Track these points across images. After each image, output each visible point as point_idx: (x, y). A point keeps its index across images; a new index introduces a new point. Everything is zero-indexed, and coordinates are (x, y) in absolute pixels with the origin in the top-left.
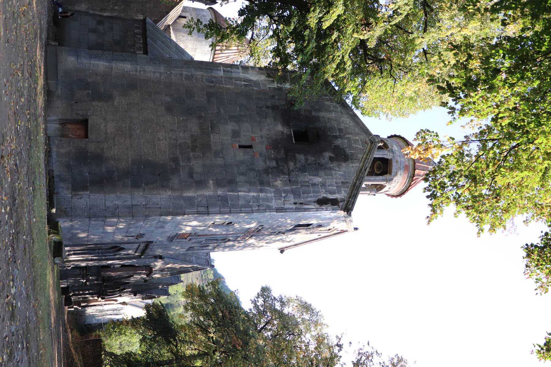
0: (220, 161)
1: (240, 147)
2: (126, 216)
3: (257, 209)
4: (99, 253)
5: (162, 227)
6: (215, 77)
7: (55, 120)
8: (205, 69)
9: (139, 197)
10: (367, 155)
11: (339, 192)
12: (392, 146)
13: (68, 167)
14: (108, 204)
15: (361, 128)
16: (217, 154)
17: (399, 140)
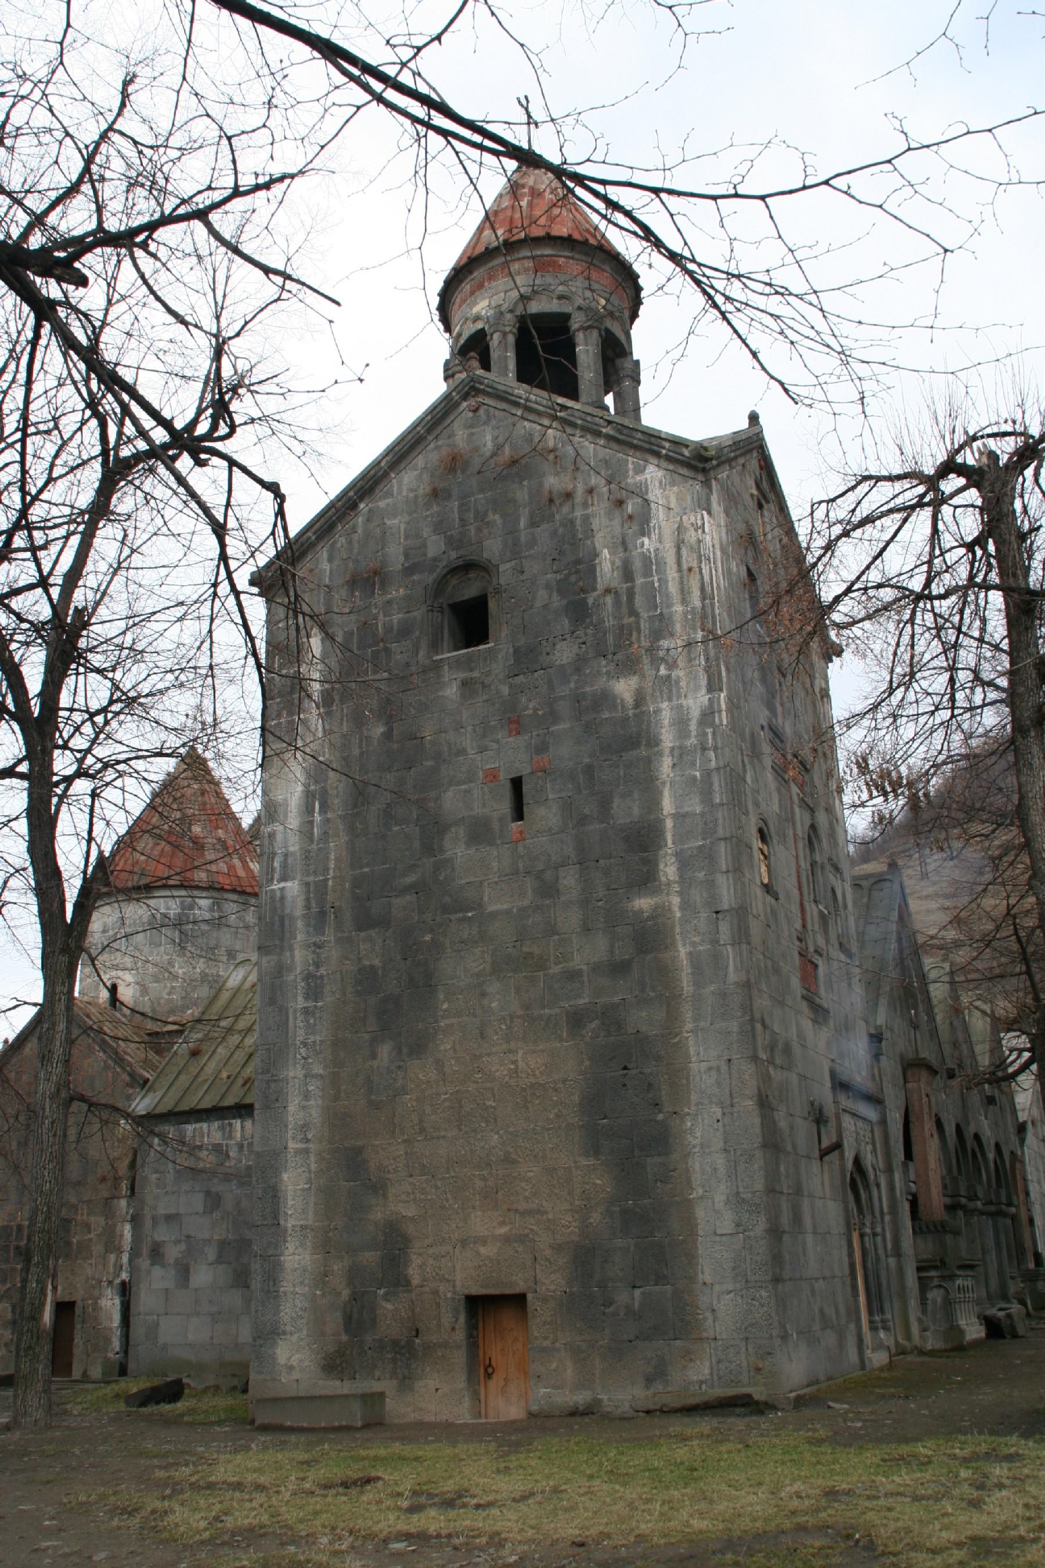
0: (569, 880)
1: (519, 814)
3: (712, 754)
4: (875, 1235)
5: (787, 1050)
6: (308, 907)
8: (282, 939)
12: (477, 318)
14: (726, 1225)
15: (429, 431)
16: (548, 890)
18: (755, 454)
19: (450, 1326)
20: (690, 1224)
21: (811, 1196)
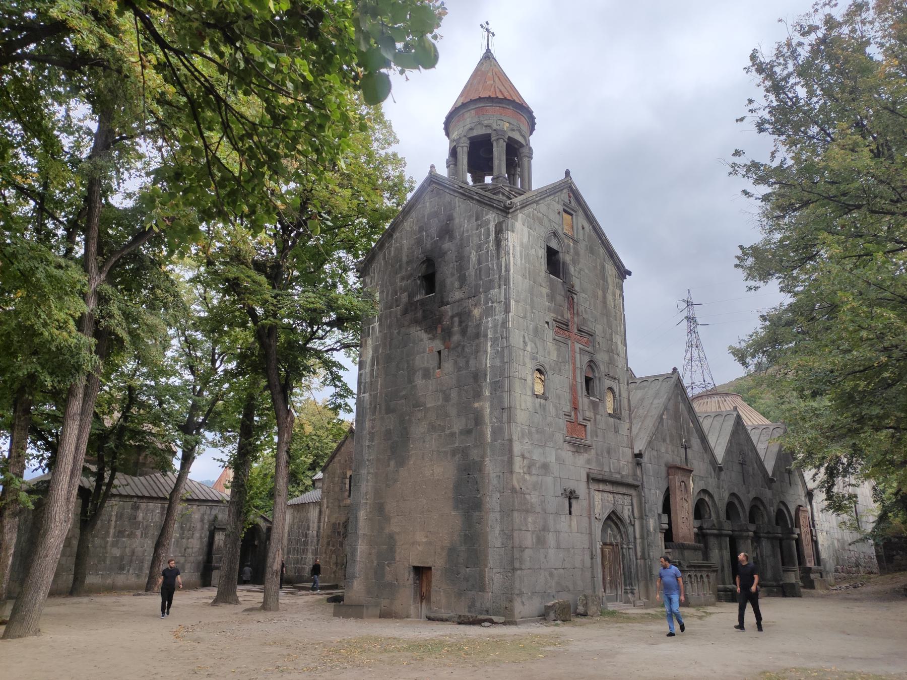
0: (454, 394)
2: (512, 520)
5: (545, 467)
6: (371, 404)
9: (493, 501)
10: (445, 187)
11: (487, 223)
12: (454, 141)
13: (460, 594)
14: (498, 544)
16: (447, 398)
17: (450, 129)
18: (565, 191)
19: (408, 578)
21: (558, 532)
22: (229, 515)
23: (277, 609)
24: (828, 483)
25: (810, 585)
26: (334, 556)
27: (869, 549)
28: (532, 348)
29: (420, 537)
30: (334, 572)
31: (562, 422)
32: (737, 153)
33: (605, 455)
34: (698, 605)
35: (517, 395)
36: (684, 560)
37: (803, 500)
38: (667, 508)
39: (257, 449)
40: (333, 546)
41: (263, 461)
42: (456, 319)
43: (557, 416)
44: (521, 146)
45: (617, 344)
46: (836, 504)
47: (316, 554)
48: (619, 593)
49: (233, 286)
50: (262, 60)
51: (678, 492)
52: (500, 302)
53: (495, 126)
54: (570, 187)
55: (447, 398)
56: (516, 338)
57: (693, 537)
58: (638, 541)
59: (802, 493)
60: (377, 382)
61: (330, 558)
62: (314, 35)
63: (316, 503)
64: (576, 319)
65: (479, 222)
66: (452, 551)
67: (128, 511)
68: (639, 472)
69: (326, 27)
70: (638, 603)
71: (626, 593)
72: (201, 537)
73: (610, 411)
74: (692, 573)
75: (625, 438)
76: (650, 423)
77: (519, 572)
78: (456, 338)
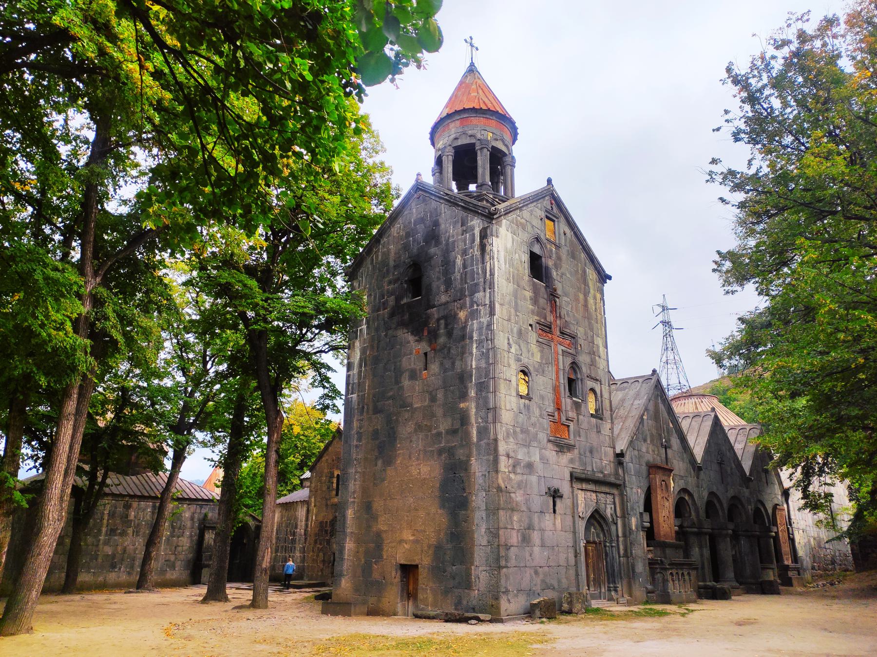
0: (440, 395)
2: (498, 518)
5: (530, 466)
6: (359, 405)
7: (404, 605)
9: (479, 500)
12: (439, 150)
13: (446, 592)
14: (484, 543)
16: (433, 399)
17: (436, 139)
18: (547, 198)
19: (395, 577)
20: (472, 539)
21: (542, 530)
22: (219, 514)
23: (266, 607)
24: (804, 482)
25: (788, 582)
26: (321, 554)
27: (845, 547)
28: (516, 350)
29: (408, 535)
30: (322, 570)
31: (546, 422)
32: (714, 161)
33: (588, 454)
34: (680, 603)
35: (502, 396)
36: (665, 558)
37: (779, 498)
38: (648, 506)
39: (247, 449)
40: (320, 544)
41: (254, 460)
42: (442, 322)
43: (541, 415)
44: (504, 154)
45: (598, 347)
46: (813, 503)
47: (304, 552)
48: (603, 590)
49: (223, 290)
50: (261, 60)
51: (659, 491)
52: (485, 305)
53: (479, 136)
54: (552, 195)
55: (433, 399)
56: (501, 340)
57: (674, 535)
58: (621, 539)
59: (779, 492)
60: (364, 383)
61: (318, 556)
62: (312, 37)
63: (303, 502)
64: (558, 322)
65: (464, 228)
66: (438, 549)
67: (120, 509)
68: (620, 471)
69: (326, 29)
70: (621, 600)
71: (609, 590)
72: (191, 536)
73: (592, 412)
74: (674, 572)
75: (607, 438)
76: (631, 424)
77: (504, 570)
78: (442, 340)
